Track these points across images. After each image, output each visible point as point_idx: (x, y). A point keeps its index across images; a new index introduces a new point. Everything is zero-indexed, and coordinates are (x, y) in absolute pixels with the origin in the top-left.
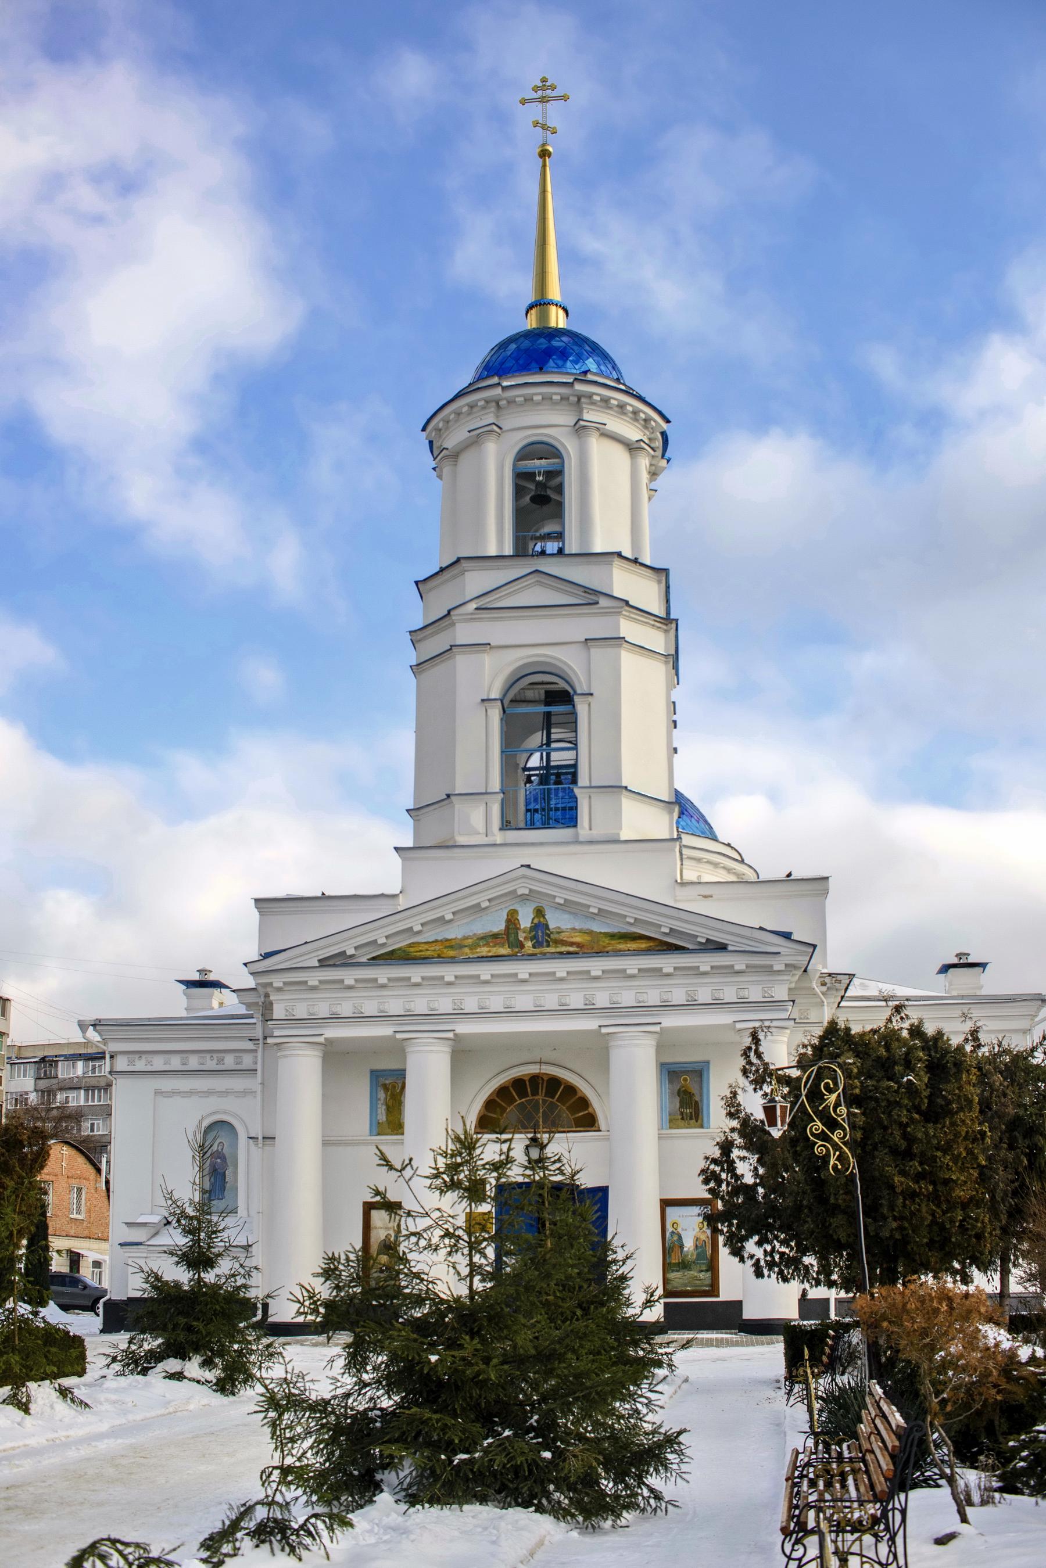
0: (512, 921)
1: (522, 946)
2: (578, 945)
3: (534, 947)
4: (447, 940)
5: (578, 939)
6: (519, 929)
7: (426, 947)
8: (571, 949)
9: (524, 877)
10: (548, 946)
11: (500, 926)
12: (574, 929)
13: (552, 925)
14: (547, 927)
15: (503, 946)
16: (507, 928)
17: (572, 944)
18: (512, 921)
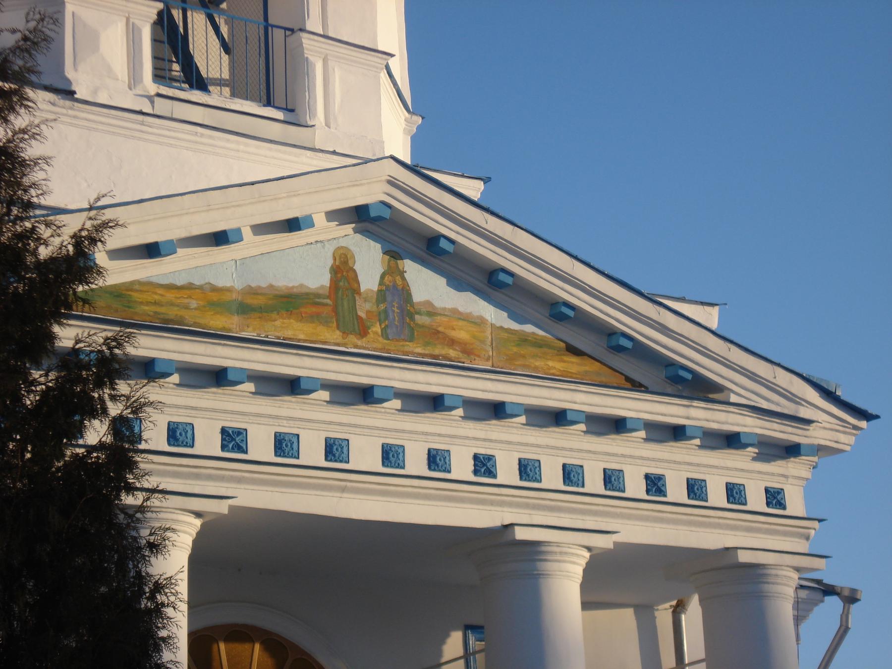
0: (343, 270)
1: (363, 332)
2: (468, 351)
3: (385, 334)
4: (215, 289)
5: (462, 335)
6: (359, 293)
7: (170, 296)
8: (452, 353)
9: (393, 183)
10: (411, 339)
11: (316, 277)
12: (455, 311)
13: (419, 295)
14: (404, 293)
15: (326, 323)
16: (334, 282)
17: (452, 342)
18: (343, 270)
